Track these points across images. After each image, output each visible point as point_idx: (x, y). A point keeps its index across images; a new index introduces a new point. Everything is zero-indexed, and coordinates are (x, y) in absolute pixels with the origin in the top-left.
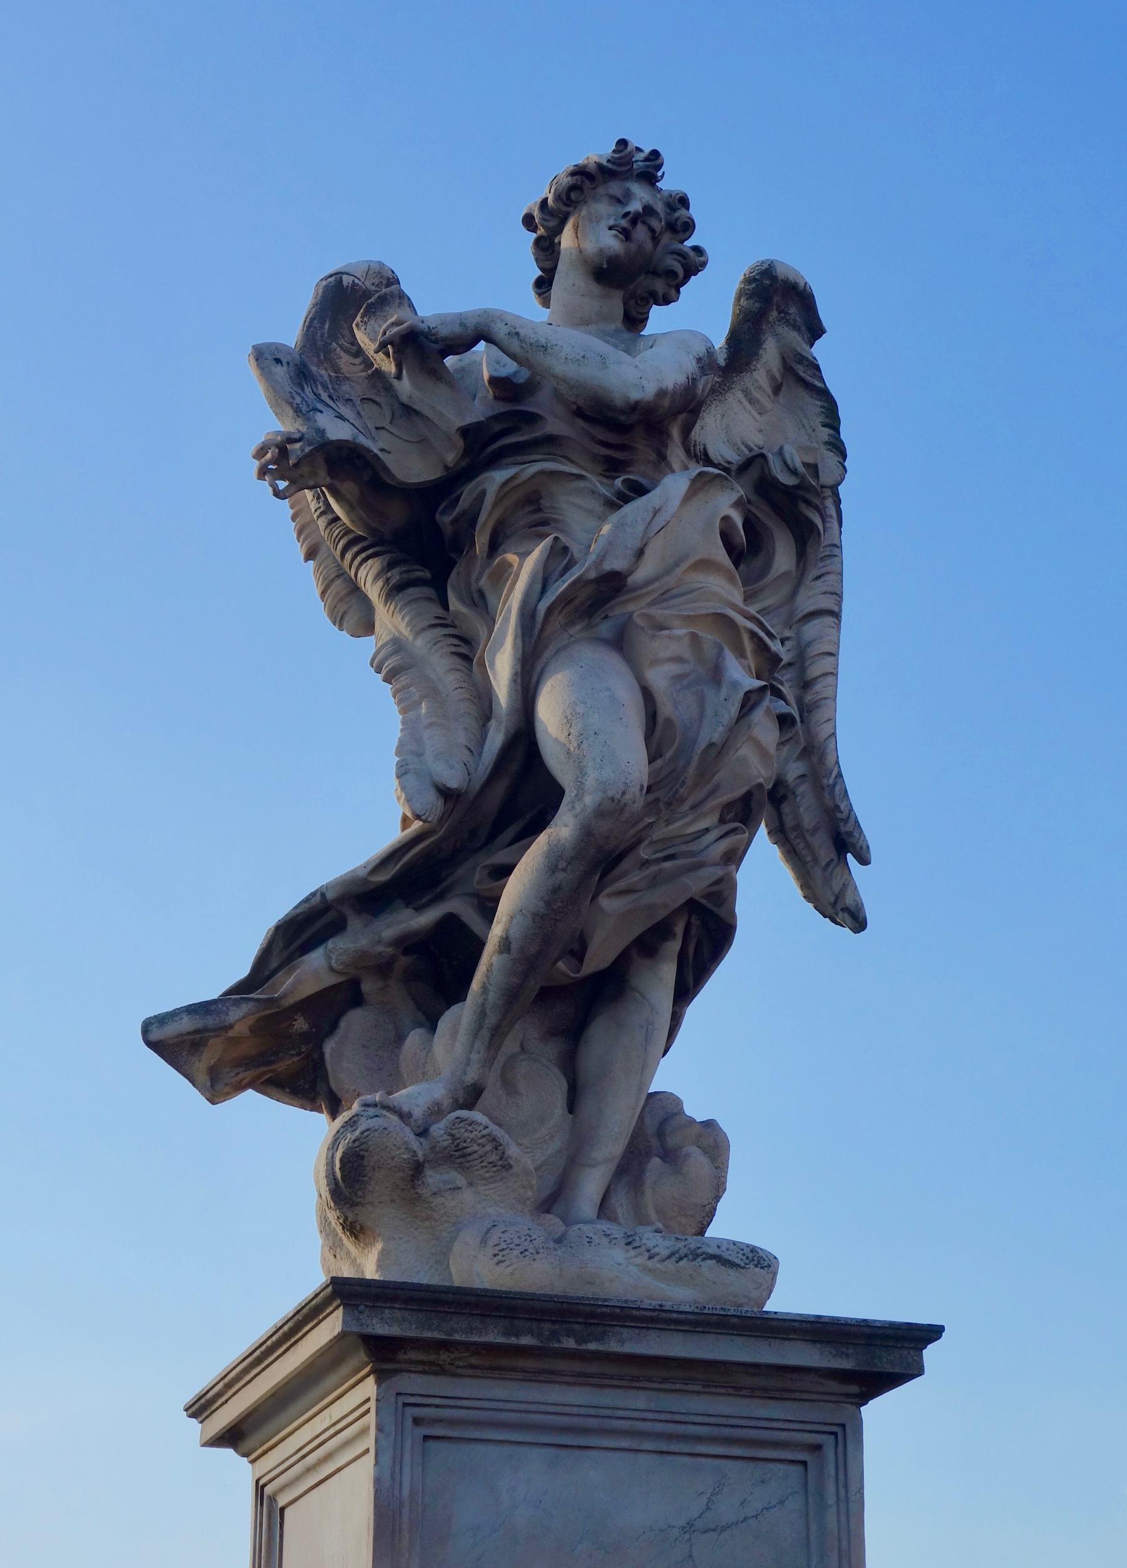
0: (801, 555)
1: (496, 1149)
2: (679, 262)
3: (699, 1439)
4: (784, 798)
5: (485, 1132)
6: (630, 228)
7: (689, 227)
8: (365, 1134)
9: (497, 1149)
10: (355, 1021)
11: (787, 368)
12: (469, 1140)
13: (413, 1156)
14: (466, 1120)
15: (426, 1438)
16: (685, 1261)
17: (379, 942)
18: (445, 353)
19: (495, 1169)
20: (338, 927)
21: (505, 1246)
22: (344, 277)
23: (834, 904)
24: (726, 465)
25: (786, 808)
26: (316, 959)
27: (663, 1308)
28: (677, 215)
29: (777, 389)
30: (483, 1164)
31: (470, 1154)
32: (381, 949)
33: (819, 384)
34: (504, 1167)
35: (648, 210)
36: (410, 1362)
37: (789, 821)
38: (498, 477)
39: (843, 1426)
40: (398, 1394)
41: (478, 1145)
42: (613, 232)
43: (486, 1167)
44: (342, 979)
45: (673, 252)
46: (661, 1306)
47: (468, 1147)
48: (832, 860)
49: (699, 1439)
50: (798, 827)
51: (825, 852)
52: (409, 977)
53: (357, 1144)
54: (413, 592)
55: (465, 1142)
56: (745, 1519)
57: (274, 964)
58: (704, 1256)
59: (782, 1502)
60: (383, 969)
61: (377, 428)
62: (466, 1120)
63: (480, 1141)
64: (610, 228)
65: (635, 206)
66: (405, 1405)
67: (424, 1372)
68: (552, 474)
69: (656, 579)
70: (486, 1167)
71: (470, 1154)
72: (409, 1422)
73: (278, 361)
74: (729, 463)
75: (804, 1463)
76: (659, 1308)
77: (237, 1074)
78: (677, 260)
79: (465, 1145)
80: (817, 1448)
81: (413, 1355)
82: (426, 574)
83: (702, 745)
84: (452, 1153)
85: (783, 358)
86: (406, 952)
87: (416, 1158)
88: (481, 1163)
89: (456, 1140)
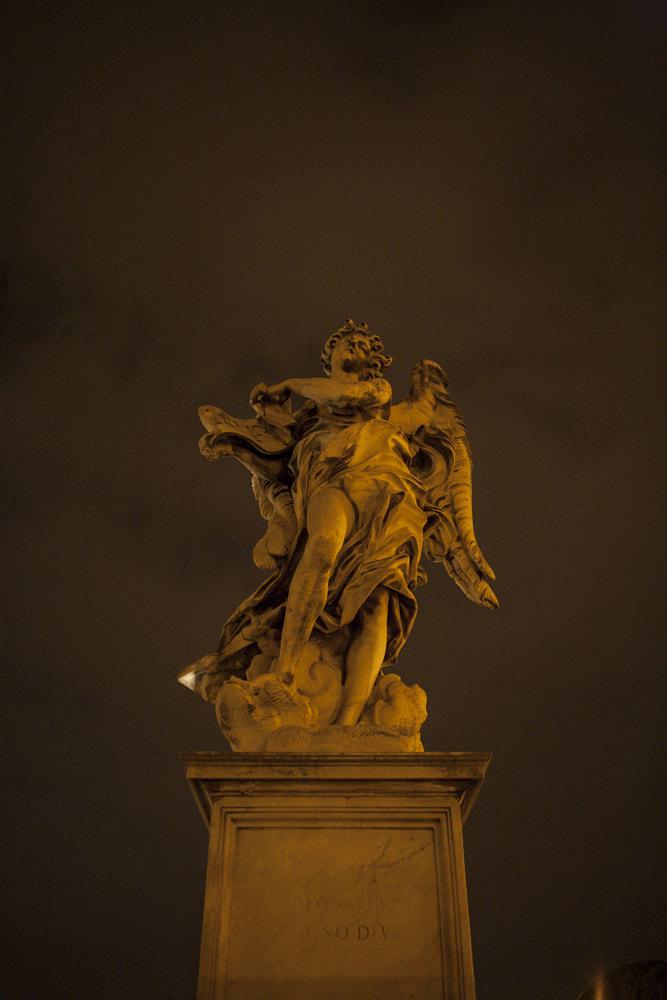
0: (448, 464)
3: (376, 820)
15: (240, 829)
23: (481, 598)
25: (453, 561)
36: (227, 791)
37: (456, 566)
39: (449, 808)
40: (222, 808)
49: (376, 820)
54: (282, 494)
56: (403, 859)
59: (422, 849)
66: (227, 813)
67: (235, 796)
72: (229, 821)
75: (432, 829)
80: (438, 821)
81: (227, 788)
82: (286, 487)
86: (272, 627)
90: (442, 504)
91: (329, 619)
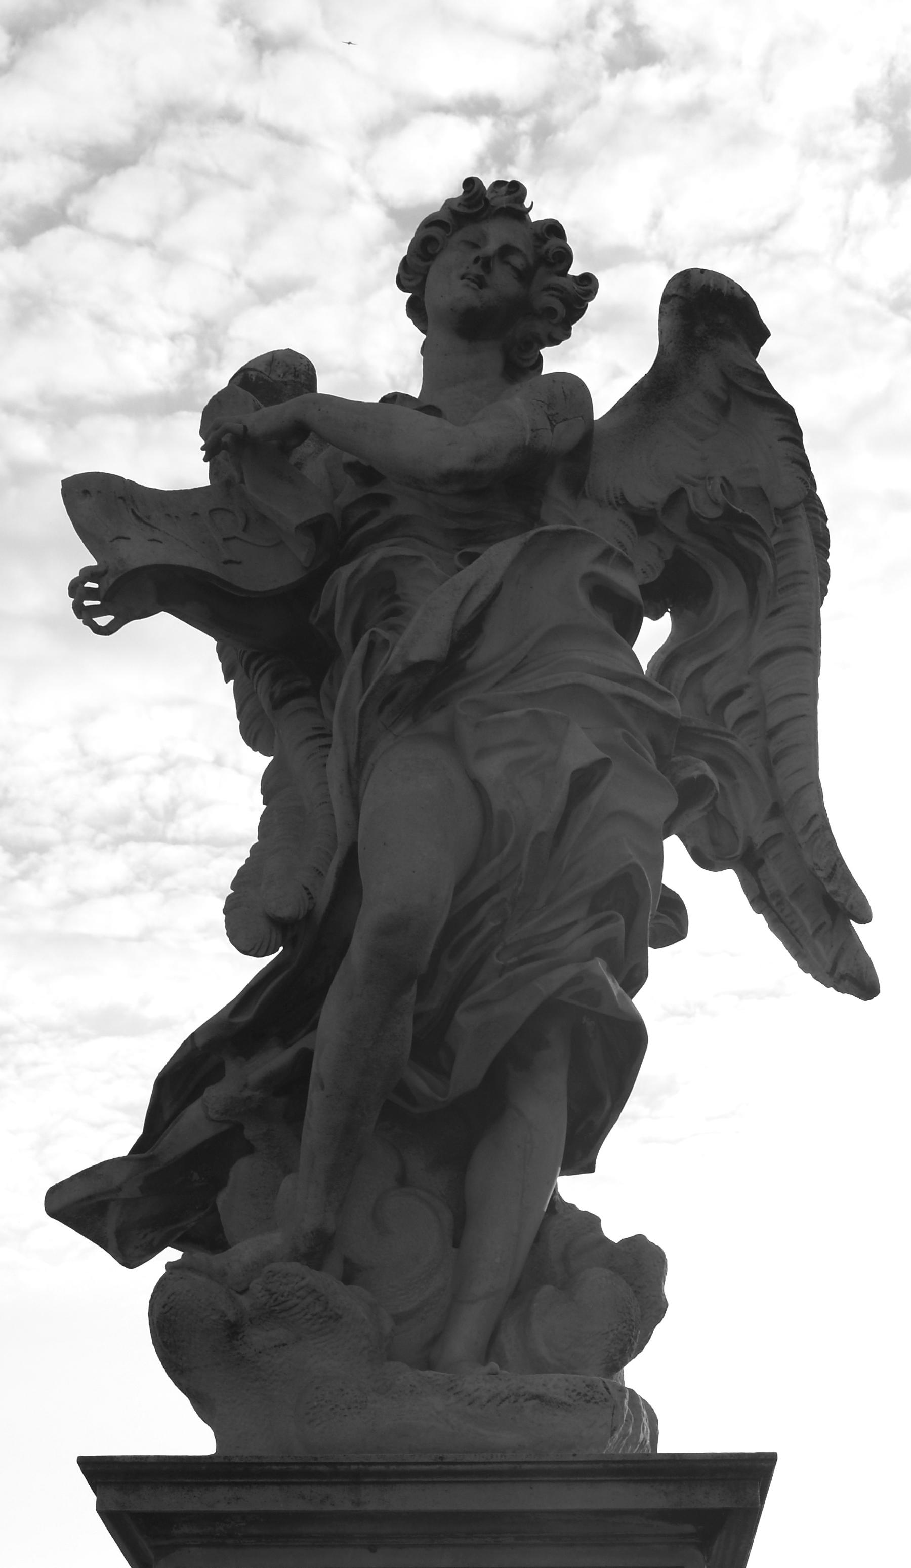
1: (318, 1299)
2: (557, 297)
5: (303, 1283)
6: (482, 273)
7: (566, 257)
8: (172, 1298)
9: (319, 1300)
11: (730, 385)
12: (286, 1294)
13: (221, 1316)
14: (279, 1273)
16: (506, 1403)
17: (246, 1086)
19: (321, 1321)
20: (216, 1074)
21: (315, 1404)
22: (251, 372)
24: (652, 507)
26: (194, 1111)
27: (445, 1460)
28: (546, 247)
29: (724, 408)
30: (308, 1317)
31: (291, 1308)
32: (247, 1093)
33: (769, 395)
34: (331, 1318)
35: (506, 250)
38: (345, 572)
41: (298, 1297)
42: (465, 281)
43: (310, 1319)
44: (225, 1127)
45: (549, 288)
46: (441, 1458)
47: (287, 1301)
48: (825, 923)
53: (167, 1308)
54: (293, 704)
55: (283, 1296)
57: (167, 1116)
58: (527, 1396)
61: (225, 539)
62: (279, 1273)
63: (298, 1294)
64: (463, 278)
65: (492, 247)
68: (396, 558)
70: (310, 1319)
71: (291, 1308)
73: (86, 492)
74: (653, 503)
76: (440, 1461)
77: (145, 1235)
78: (553, 295)
79: (283, 1299)
84: (273, 1308)
85: (724, 375)
87: (226, 1319)
88: (304, 1316)
89: (273, 1294)
90: (734, 710)
91: (420, 1082)
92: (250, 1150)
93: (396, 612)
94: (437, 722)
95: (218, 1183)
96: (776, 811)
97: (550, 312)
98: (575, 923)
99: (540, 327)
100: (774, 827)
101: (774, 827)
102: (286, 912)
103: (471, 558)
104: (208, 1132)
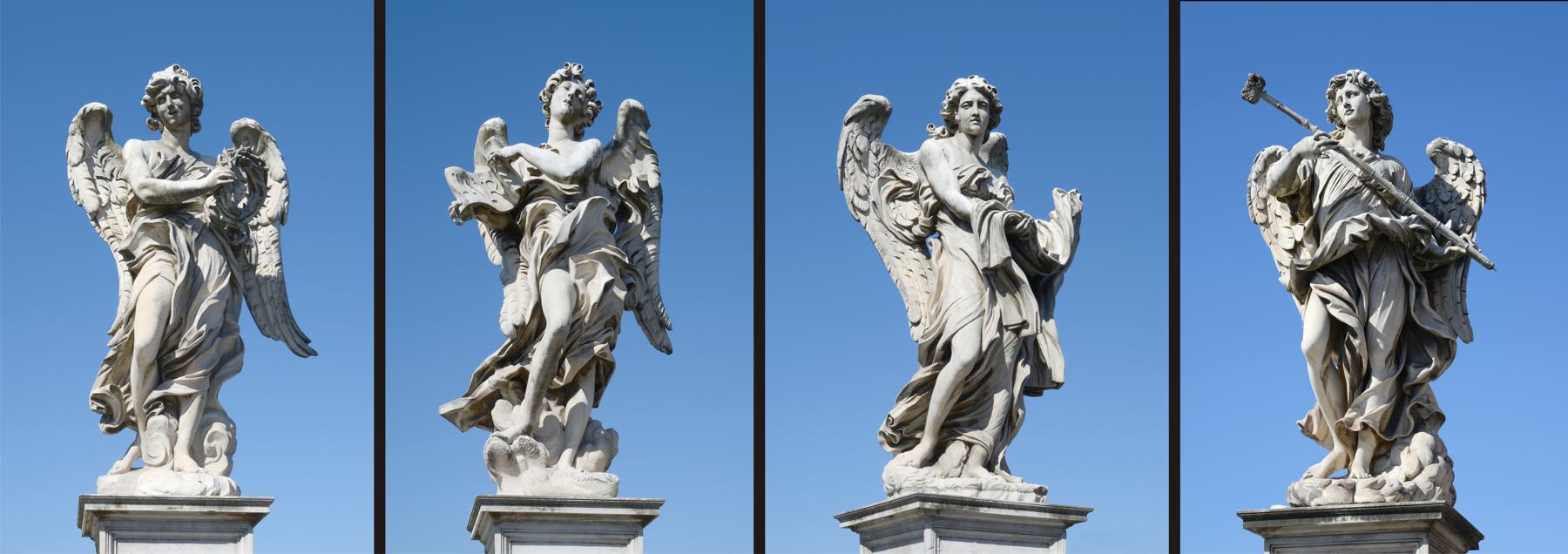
4: (641, 309)
10: (499, 403)
18: (511, 161)
20: (492, 373)
37: (644, 317)
38: (529, 207)
50: (646, 319)
51: (656, 327)
52: (514, 388)
60: (505, 385)
69: (580, 241)
83: (592, 304)
86: (512, 380)
90: (636, 258)
92: (501, 397)
93: (545, 223)
94: (562, 263)
95: (492, 406)
96: (648, 291)
97: (589, 114)
98: (600, 331)
99: (586, 120)
100: (646, 297)
101: (646, 297)
102: (518, 324)
103: (573, 208)
104: (491, 391)
